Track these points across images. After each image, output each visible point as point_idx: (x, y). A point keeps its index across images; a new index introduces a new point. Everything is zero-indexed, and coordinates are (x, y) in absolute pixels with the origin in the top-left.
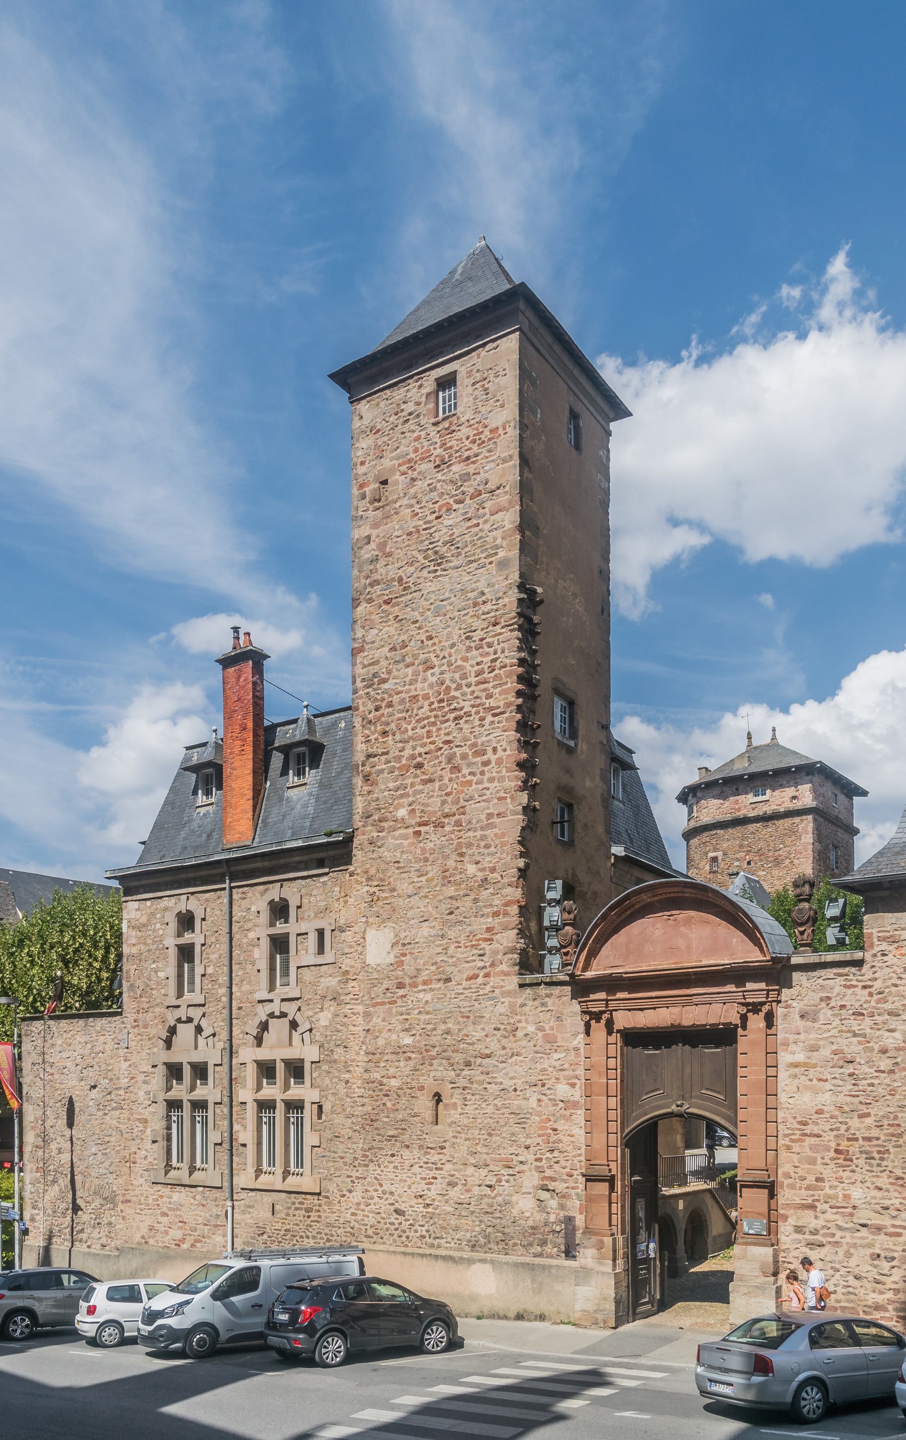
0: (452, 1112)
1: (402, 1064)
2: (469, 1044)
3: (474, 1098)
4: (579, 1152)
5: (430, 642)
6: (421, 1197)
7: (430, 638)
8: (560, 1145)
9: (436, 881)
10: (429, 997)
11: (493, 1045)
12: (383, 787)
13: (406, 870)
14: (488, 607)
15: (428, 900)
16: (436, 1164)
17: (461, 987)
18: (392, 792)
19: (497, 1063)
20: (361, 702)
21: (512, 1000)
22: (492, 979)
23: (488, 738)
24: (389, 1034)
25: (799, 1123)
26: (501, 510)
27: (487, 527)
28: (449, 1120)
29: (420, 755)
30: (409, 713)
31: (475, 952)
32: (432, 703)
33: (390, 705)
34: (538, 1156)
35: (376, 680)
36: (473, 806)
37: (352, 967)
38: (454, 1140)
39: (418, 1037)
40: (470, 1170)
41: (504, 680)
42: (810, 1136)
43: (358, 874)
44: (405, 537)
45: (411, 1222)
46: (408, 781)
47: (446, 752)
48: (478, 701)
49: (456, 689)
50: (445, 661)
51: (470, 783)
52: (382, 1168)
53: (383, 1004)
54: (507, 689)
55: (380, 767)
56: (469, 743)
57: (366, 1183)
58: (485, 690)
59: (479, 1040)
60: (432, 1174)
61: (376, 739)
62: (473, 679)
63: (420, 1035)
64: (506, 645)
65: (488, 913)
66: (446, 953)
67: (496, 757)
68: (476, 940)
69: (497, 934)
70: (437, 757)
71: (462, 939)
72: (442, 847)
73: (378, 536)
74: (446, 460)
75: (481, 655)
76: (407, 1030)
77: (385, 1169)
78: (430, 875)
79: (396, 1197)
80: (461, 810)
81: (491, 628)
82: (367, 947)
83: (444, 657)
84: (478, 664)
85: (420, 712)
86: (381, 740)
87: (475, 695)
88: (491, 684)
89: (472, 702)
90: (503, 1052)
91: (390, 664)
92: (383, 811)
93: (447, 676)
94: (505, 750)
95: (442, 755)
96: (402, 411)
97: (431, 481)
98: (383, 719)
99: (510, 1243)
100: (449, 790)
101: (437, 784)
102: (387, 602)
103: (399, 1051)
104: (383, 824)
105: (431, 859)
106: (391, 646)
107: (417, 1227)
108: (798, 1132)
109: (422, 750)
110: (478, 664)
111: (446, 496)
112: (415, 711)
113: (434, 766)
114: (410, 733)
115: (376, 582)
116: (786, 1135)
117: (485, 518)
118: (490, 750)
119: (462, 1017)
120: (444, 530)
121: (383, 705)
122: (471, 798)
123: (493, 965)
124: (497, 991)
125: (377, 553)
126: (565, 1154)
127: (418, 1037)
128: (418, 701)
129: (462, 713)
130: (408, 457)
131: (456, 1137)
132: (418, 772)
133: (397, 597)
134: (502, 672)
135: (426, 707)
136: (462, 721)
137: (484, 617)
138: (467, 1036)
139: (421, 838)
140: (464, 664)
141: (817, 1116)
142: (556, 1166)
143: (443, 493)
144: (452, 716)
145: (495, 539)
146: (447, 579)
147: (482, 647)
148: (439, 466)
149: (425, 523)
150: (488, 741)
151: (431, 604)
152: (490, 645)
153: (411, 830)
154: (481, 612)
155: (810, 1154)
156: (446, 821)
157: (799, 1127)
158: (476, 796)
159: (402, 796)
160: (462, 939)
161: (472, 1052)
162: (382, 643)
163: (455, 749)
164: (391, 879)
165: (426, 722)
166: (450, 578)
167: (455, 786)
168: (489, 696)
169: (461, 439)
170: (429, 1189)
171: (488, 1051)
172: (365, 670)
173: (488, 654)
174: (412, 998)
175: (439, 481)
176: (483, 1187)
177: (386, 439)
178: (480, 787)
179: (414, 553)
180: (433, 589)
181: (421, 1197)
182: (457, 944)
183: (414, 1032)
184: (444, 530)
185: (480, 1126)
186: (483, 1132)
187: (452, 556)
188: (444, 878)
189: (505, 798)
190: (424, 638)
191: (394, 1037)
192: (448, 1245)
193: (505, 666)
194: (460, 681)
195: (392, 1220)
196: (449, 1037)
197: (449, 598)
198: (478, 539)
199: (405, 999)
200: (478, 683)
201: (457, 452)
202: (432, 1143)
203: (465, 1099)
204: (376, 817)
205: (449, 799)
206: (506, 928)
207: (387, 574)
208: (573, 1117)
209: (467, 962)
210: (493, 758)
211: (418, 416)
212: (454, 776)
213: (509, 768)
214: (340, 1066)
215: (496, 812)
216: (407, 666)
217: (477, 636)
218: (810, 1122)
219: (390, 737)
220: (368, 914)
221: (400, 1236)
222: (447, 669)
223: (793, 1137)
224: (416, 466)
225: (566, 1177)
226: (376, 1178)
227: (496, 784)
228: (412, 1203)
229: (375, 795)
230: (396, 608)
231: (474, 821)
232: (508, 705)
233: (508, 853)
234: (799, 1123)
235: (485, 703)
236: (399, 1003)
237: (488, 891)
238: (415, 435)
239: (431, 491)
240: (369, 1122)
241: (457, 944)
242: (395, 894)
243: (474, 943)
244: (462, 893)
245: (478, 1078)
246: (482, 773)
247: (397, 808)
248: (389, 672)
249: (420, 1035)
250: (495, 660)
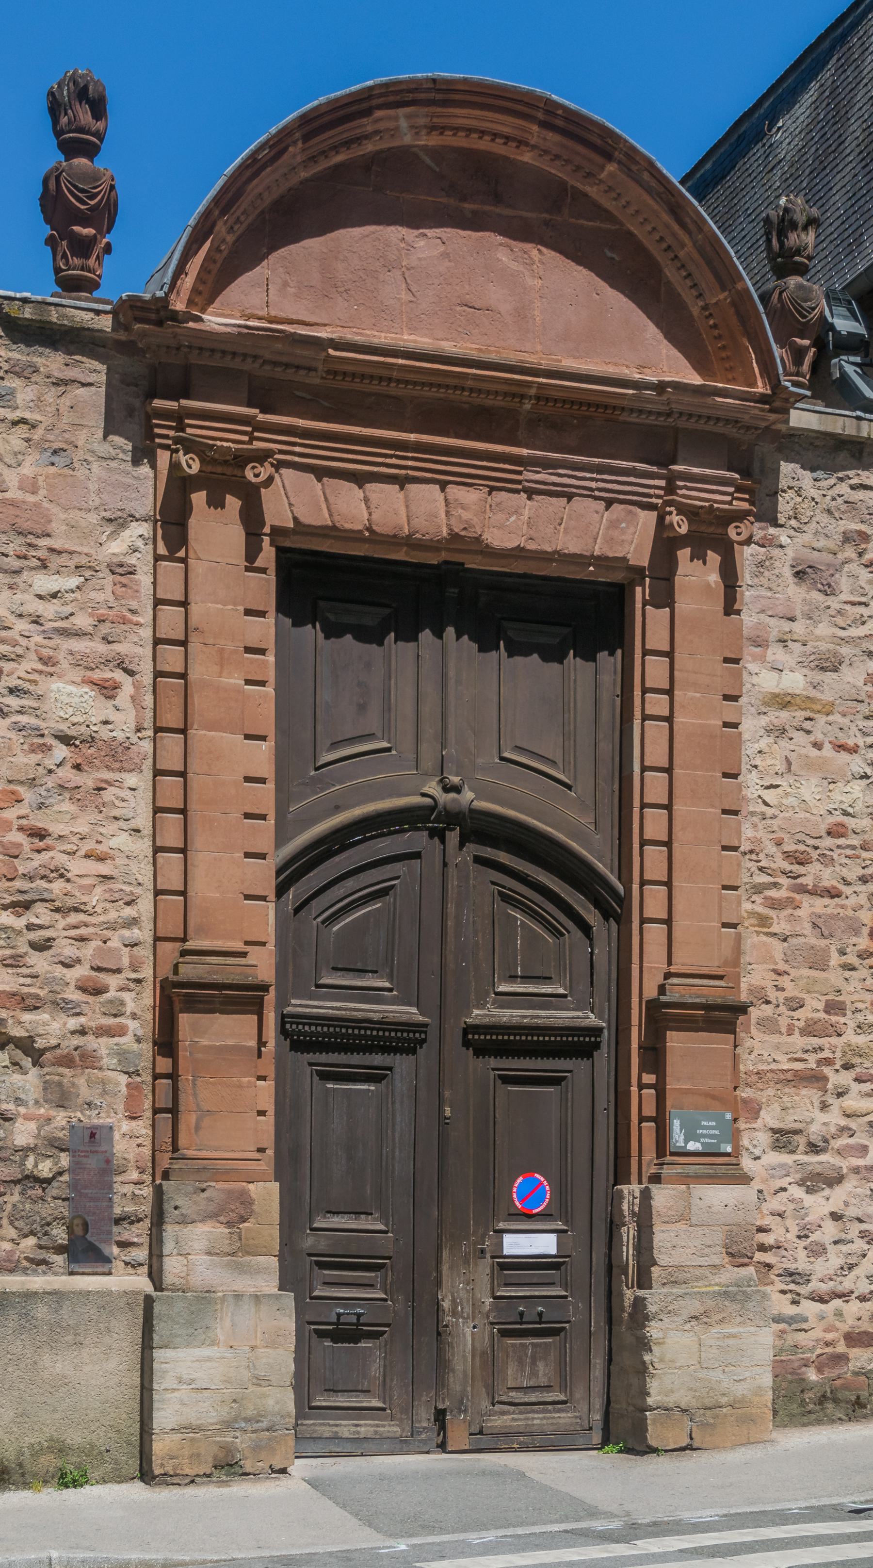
4: (128, 912)
8: (58, 887)
25: (787, 855)
42: (812, 893)
108: (783, 881)
116: (758, 889)
126: (74, 918)
141: (829, 842)
155: (813, 941)
157: (787, 867)
208: (109, 795)
218: (815, 854)
223: (773, 893)
225: (74, 996)
234: (787, 855)
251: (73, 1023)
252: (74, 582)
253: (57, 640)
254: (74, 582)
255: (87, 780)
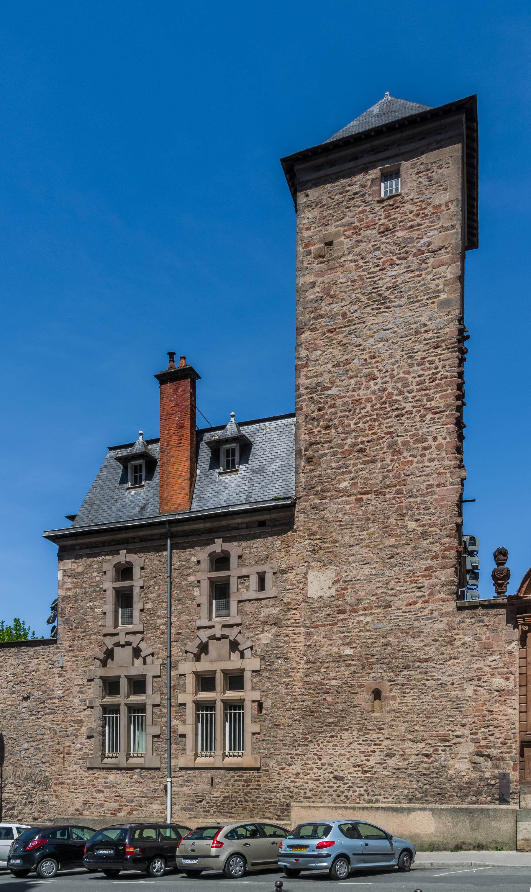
0: (391, 702)
1: (342, 669)
2: (409, 652)
3: (412, 691)
5: (373, 361)
6: (359, 766)
7: (374, 357)
8: (495, 722)
9: (377, 535)
10: (369, 619)
11: (432, 651)
12: (326, 466)
13: (348, 526)
14: (431, 335)
15: (369, 549)
16: (375, 741)
17: (401, 611)
18: (335, 470)
19: (435, 665)
20: (304, 404)
21: (450, 619)
22: (431, 604)
23: (428, 430)
24: (331, 647)
26: (443, 265)
27: (430, 277)
28: (388, 709)
29: (362, 442)
30: (352, 412)
31: (415, 585)
32: (375, 405)
33: (332, 406)
34: (474, 731)
35: (319, 388)
36: (413, 479)
37: (294, 599)
38: (393, 723)
39: (358, 649)
40: (409, 744)
41: (445, 388)
43: (300, 531)
44: (349, 283)
45: (350, 784)
46: (351, 462)
47: (387, 441)
48: (419, 403)
49: (398, 395)
50: (388, 374)
51: (411, 463)
52: (322, 746)
53: (324, 625)
54: (448, 394)
55: (323, 452)
56: (409, 434)
57: (305, 758)
58: (426, 395)
59: (418, 649)
60: (370, 749)
61: (319, 431)
62: (415, 388)
63: (361, 647)
64: (447, 362)
65: (427, 556)
66: (386, 587)
67: (436, 443)
68: (416, 576)
69: (436, 572)
70: (379, 444)
71: (402, 577)
72: (385, 509)
73: (322, 283)
74: (391, 228)
75: (423, 370)
76: (347, 644)
77: (324, 747)
78: (371, 530)
79: (335, 767)
80: (403, 483)
81: (432, 350)
82: (309, 584)
83: (387, 371)
84: (419, 376)
85: (363, 411)
86: (323, 432)
87: (416, 399)
88: (432, 391)
89: (414, 404)
90: (441, 657)
91: (334, 376)
92: (325, 484)
93: (389, 386)
94: (445, 438)
95: (383, 442)
96: (348, 191)
97: (375, 243)
98: (326, 417)
99: (447, 795)
100: (391, 467)
101: (379, 464)
102: (330, 331)
103: (339, 659)
104: (325, 494)
105: (372, 519)
106: (335, 363)
107: (355, 788)
109: (365, 439)
110: (419, 376)
111: (390, 254)
112: (358, 411)
113: (376, 450)
114: (353, 426)
115: (322, 316)
117: (427, 271)
118: (430, 439)
119: (402, 633)
120: (388, 279)
121: (327, 406)
122: (412, 474)
123: (431, 594)
124: (436, 613)
125: (321, 295)
127: (358, 649)
128: (361, 403)
129: (404, 411)
130: (354, 225)
131: (395, 721)
132: (361, 455)
133: (341, 328)
134: (442, 382)
135: (369, 408)
136: (403, 418)
137: (426, 342)
138: (407, 646)
139: (363, 503)
140: (407, 376)
142: (491, 738)
143: (387, 252)
144: (394, 414)
145: (437, 285)
146: (390, 314)
147: (423, 364)
148: (383, 232)
149: (369, 274)
150: (429, 432)
151: (375, 332)
152: (431, 362)
153: (353, 498)
154: (423, 338)
156: (388, 490)
158: (417, 472)
159: (344, 473)
160: (402, 577)
161: (411, 658)
162: (326, 361)
163: (396, 438)
164: (334, 534)
165: (368, 418)
166: (393, 314)
167: (396, 465)
168: (430, 399)
169: (405, 213)
170: (368, 760)
171: (426, 657)
172: (308, 381)
173: (429, 369)
174: (352, 621)
175: (384, 243)
176: (420, 756)
177: (331, 211)
178: (421, 465)
179: (358, 295)
180: (376, 321)
181: (359, 766)
182: (397, 580)
183: (354, 645)
184: (388, 279)
185: (419, 711)
186: (421, 716)
187: (396, 297)
188: (384, 533)
189: (445, 473)
190: (367, 357)
191: (335, 649)
192: (386, 800)
193: (446, 378)
194: (402, 389)
195: (331, 784)
196: (389, 648)
197: (393, 328)
198: (420, 286)
199: (346, 622)
200: (418, 391)
201: (401, 222)
202: (371, 726)
203: (404, 693)
204: (319, 489)
205: (391, 475)
206: (444, 568)
207: (331, 311)
208: (508, 701)
209: (407, 593)
210: (433, 444)
211: (363, 195)
212: (396, 457)
213: (450, 451)
214: (282, 673)
215: (436, 483)
216: (351, 378)
217: (419, 356)
219: (333, 430)
220: (310, 559)
221: (339, 796)
222: (390, 380)
224: (361, 232)
226: (315, 754)
227: (436, 463)
228: (350, 771)
229: (318, 472)
230: (340, 336)
231: (414, 490)
232: (447, 406)
233: (447, 513)
235: (426, 404)
236: (340, 624)
237: (428, 541)
238: (360, 209)
239: (376, 250)
240: (310, 713)
241: (397, 580)
242: (337, 545)
243: (413, 579)
244: (402, 543)
245: (416, 677)
246: (423, 455)
247: (339, 482)
248: (333, 383)
249: (361, 647)
250: (437, 373)
251: (499, 751)
252: (499, 657)
253: (495, 670)
254: (499, 657)
255: (502, 699)
